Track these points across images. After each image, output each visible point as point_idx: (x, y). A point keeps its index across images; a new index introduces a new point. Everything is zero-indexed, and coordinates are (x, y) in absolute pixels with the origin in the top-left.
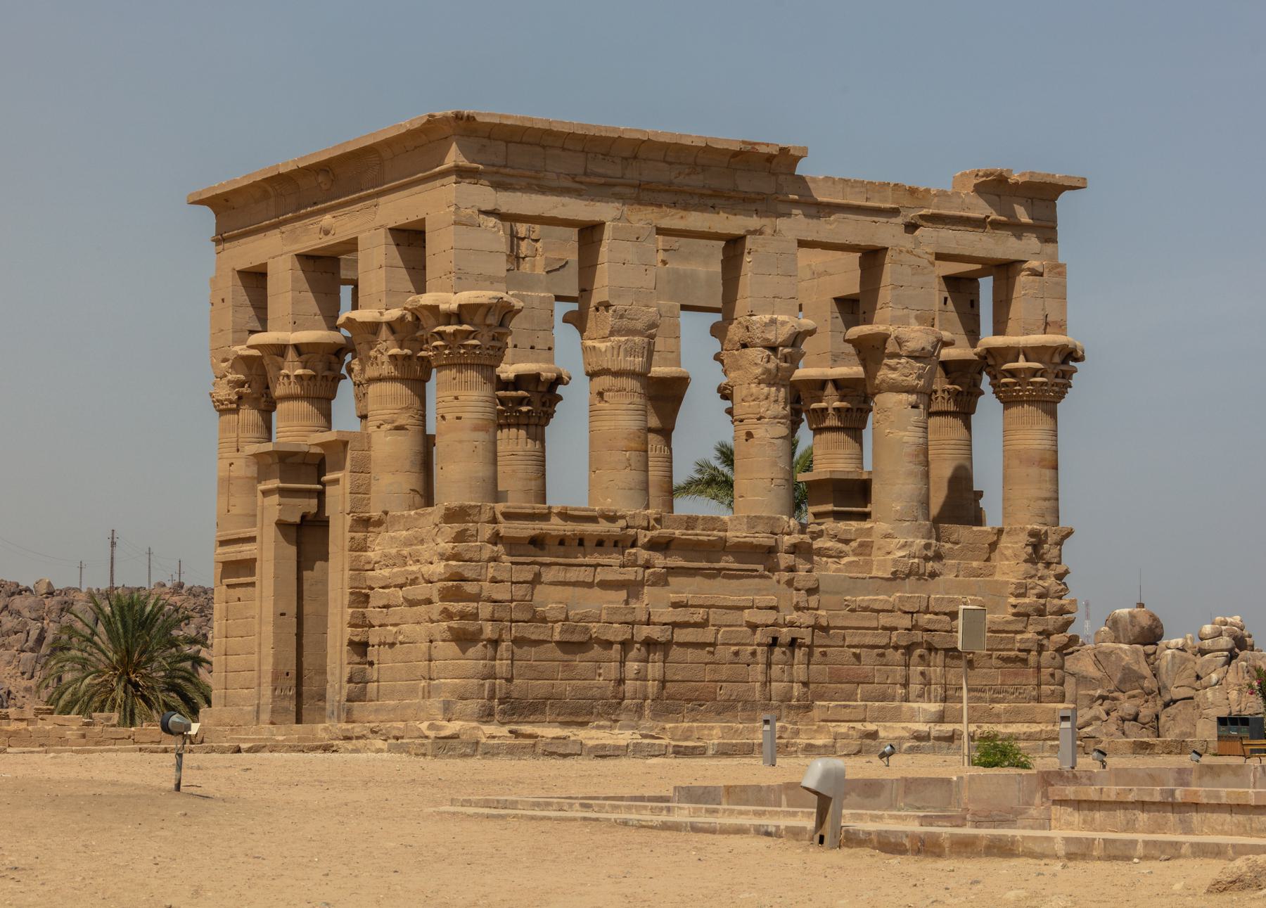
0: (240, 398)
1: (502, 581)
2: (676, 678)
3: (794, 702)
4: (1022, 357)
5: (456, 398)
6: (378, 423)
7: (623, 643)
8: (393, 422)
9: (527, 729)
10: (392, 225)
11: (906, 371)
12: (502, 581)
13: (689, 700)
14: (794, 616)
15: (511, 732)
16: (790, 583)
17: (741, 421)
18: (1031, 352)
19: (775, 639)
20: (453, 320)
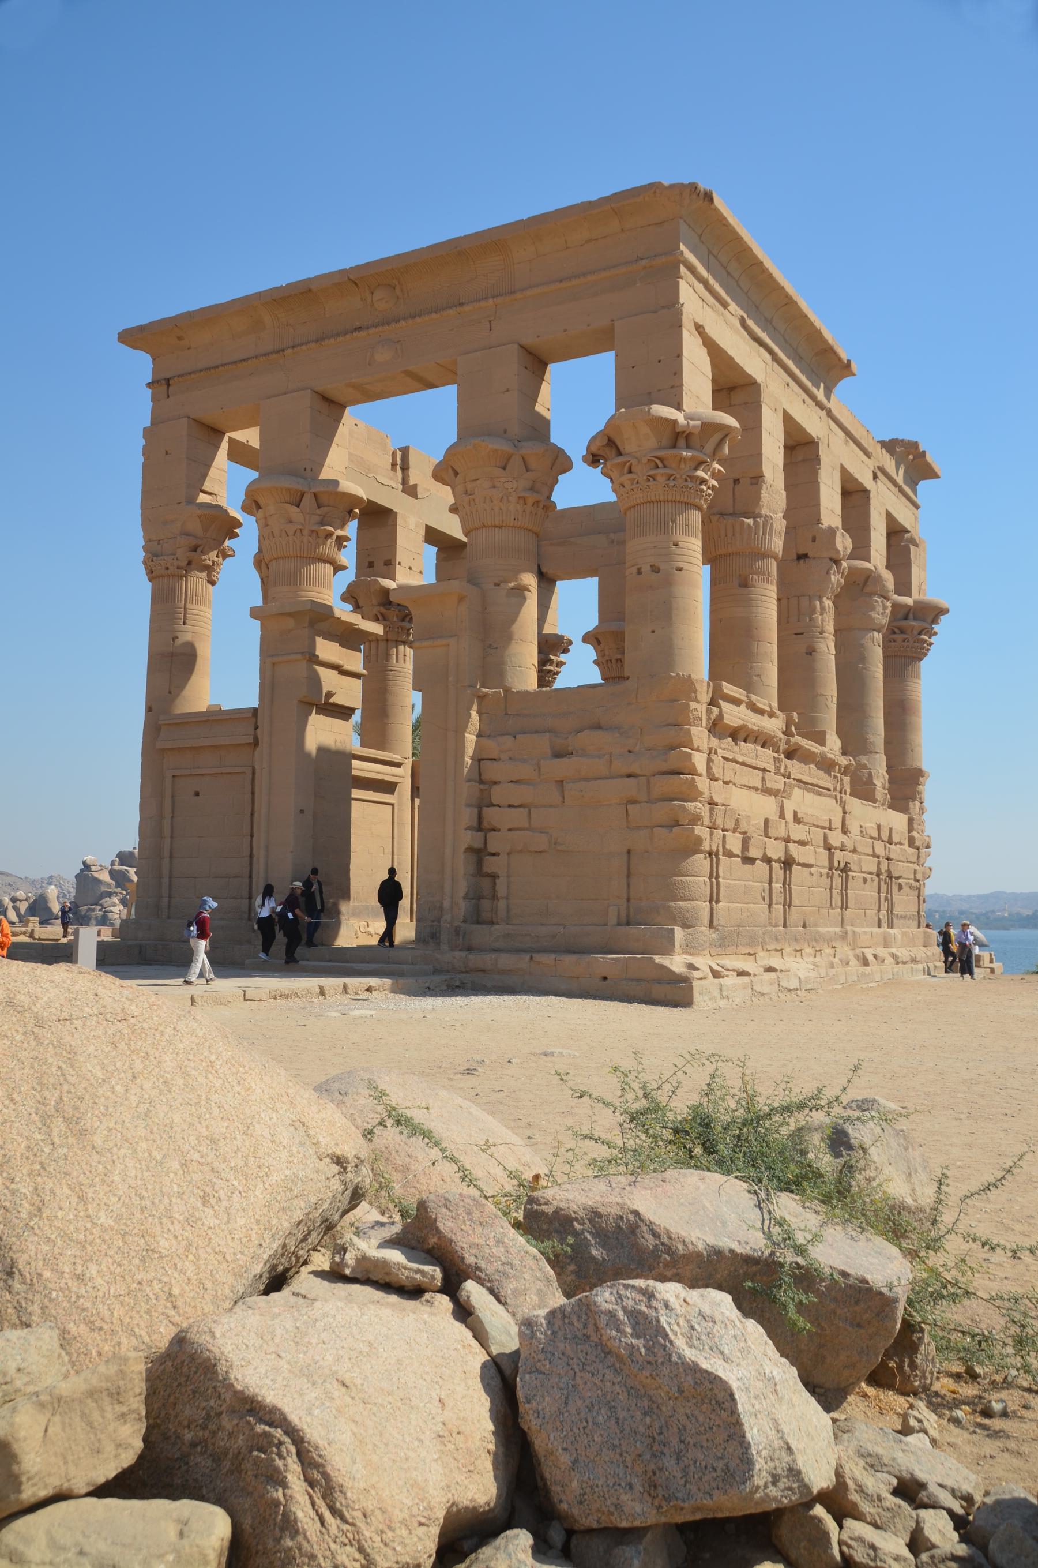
0: (189, 563)
5: (676, 545)
10: (528, 341)
20: (682, 442)
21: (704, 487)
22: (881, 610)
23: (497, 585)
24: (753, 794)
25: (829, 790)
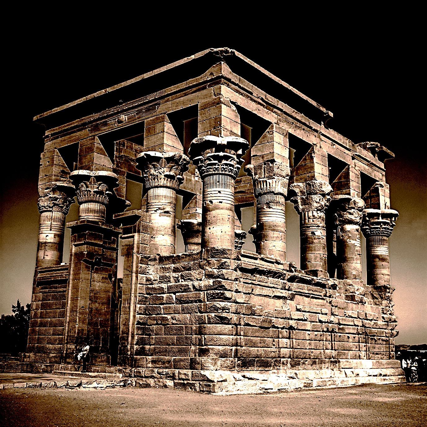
1: (240, 292)
2: (299, 347)
3: (332, 360)
4: (380, 218)
5: (219, 192)
6: (155, 209)
7: (283, 328)
8: (164, 209)
9: (247, 374)
11: (357, 215)
12: (240, 292)
13: (302, 358)
14: (332, 318)
15: (244, 376)
16: (330, 303)
17: (309, 227)
18: (384, 216)
19: (328, 329)
21: (232, 168)
22: (357, 215)
23: (155, 211)
24: (267, 299)
25: (321, 296)
